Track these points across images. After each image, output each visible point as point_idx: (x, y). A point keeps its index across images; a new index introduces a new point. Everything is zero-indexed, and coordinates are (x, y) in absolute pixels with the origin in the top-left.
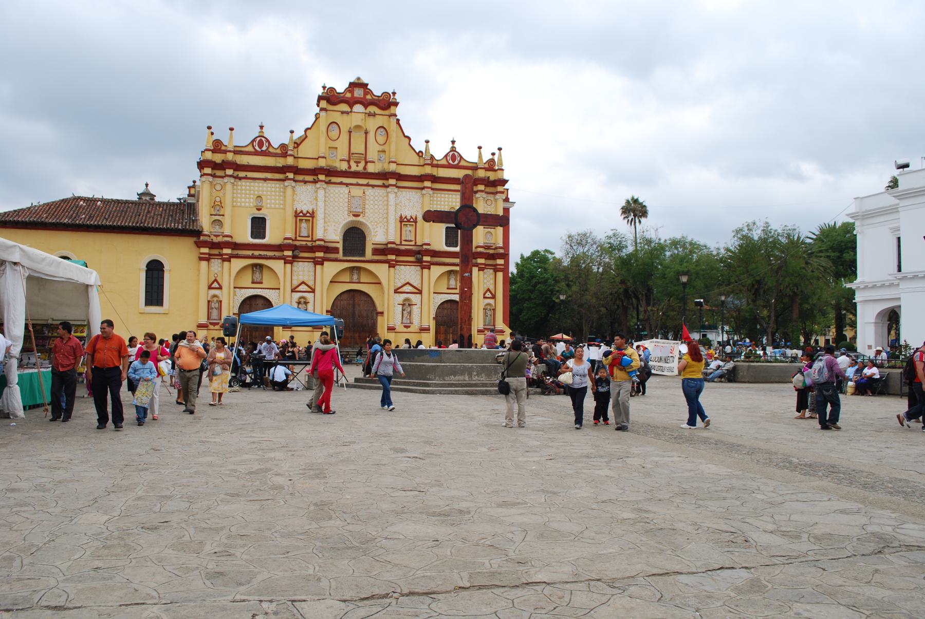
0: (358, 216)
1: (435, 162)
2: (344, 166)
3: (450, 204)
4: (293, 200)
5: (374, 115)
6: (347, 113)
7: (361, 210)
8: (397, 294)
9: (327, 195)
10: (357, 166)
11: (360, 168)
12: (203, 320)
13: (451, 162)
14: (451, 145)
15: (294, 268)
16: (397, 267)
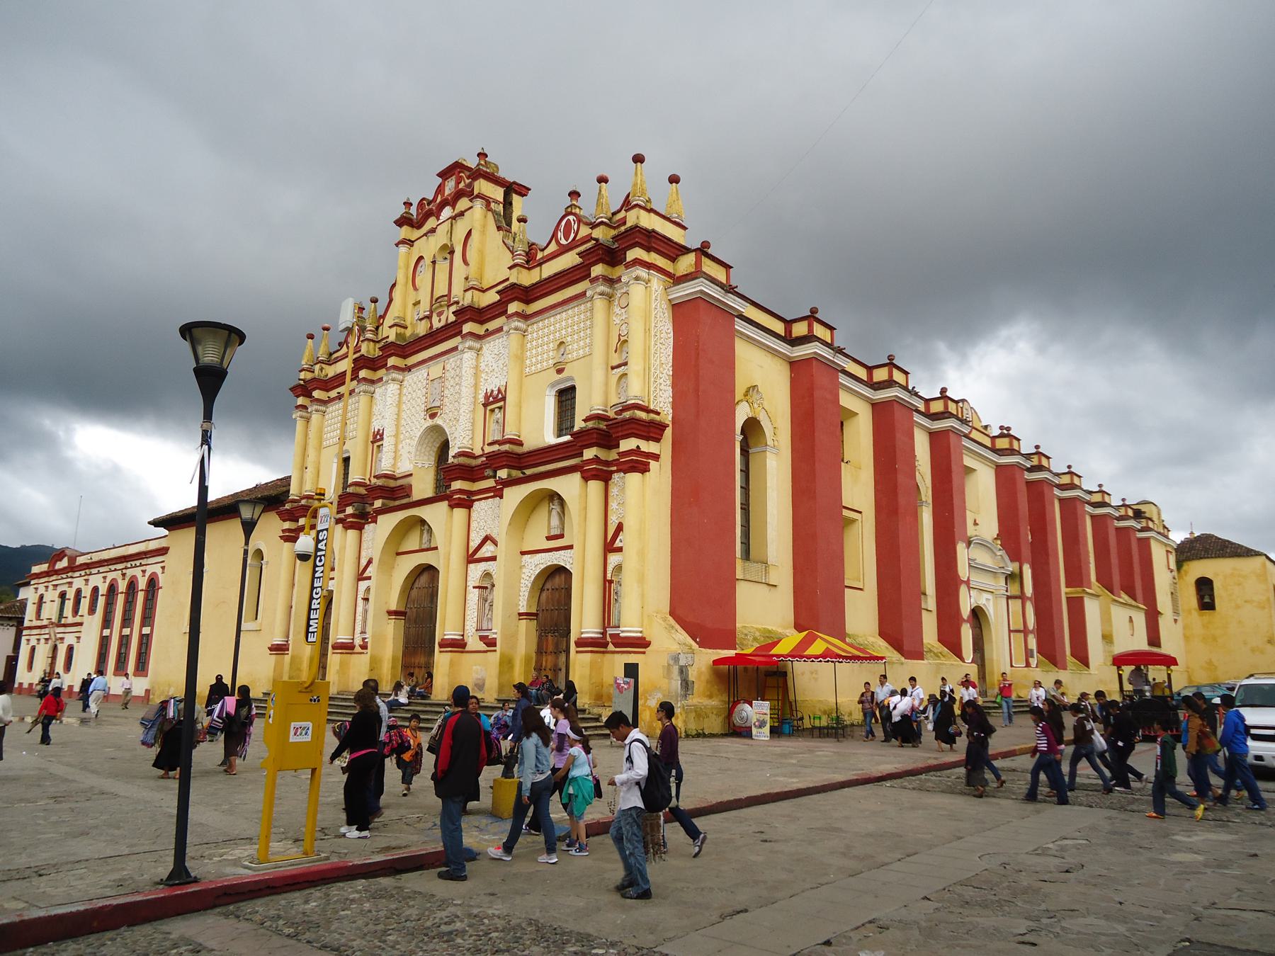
0: (433, 416)
1: (540, 255)
2: (422, 329)
3: (557, 334)
4: (370, 414)
5: (462, 214)
6: (433, 231)
7: (437, 404)
8: (472, 566)
9: (405, 391)
10: (440, 321)
11: (443, 323)
12: (278, 640)
13: (563, 242)
14: (568, 201)
15: (363, 539)
16: (476, 504)
